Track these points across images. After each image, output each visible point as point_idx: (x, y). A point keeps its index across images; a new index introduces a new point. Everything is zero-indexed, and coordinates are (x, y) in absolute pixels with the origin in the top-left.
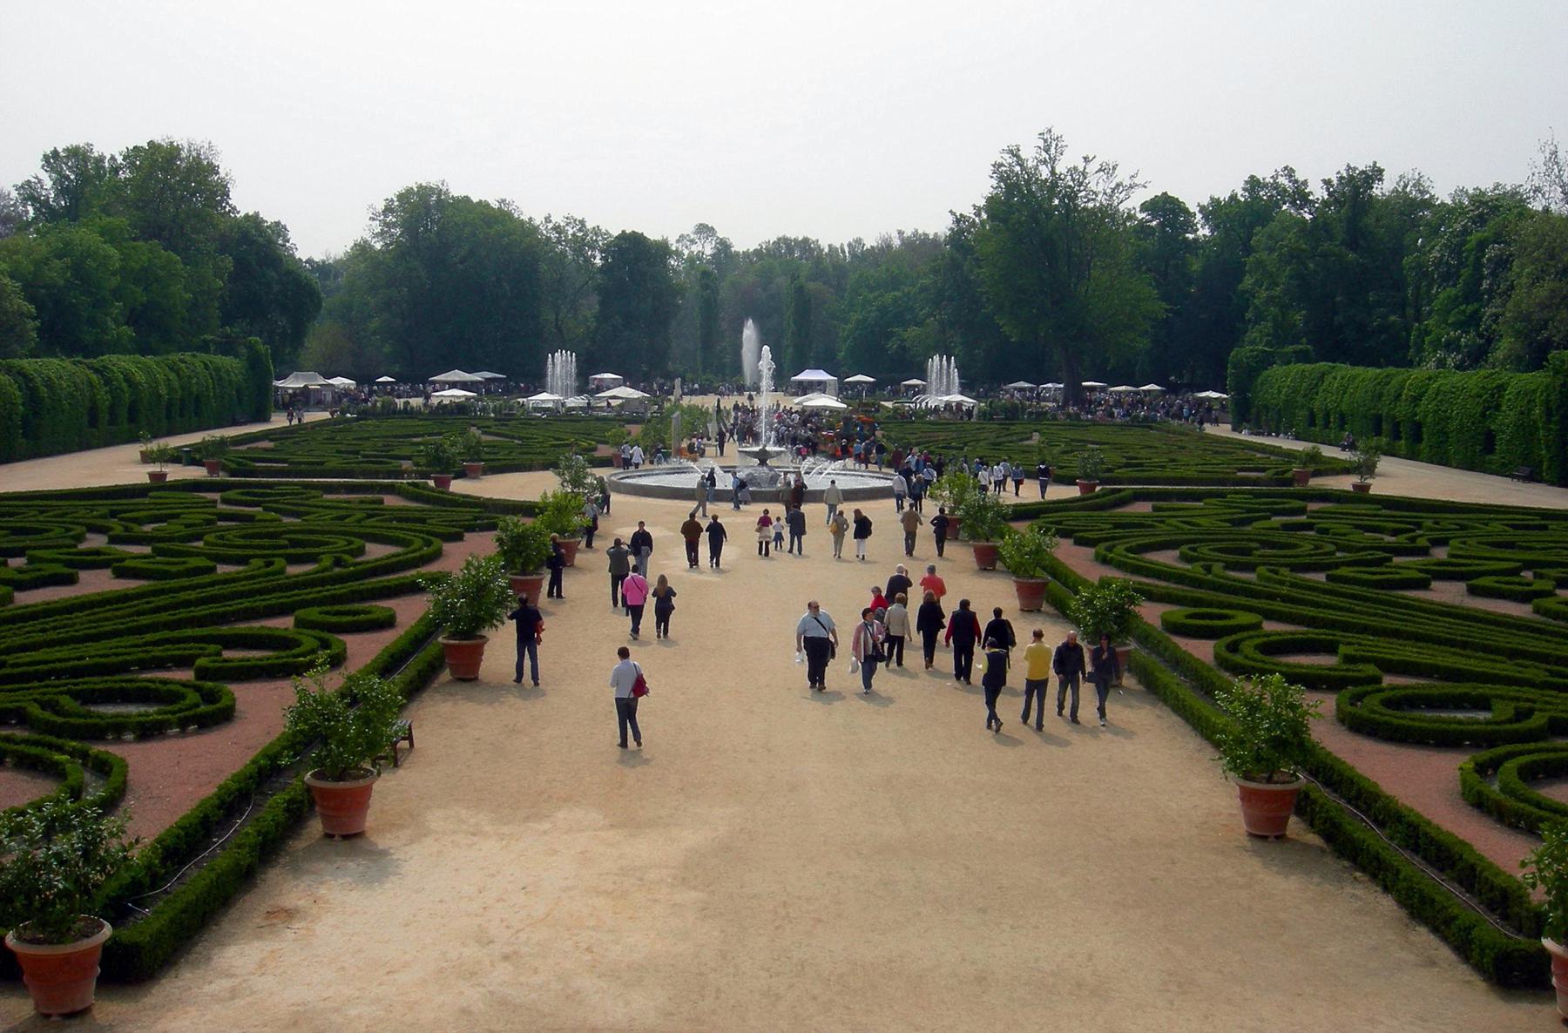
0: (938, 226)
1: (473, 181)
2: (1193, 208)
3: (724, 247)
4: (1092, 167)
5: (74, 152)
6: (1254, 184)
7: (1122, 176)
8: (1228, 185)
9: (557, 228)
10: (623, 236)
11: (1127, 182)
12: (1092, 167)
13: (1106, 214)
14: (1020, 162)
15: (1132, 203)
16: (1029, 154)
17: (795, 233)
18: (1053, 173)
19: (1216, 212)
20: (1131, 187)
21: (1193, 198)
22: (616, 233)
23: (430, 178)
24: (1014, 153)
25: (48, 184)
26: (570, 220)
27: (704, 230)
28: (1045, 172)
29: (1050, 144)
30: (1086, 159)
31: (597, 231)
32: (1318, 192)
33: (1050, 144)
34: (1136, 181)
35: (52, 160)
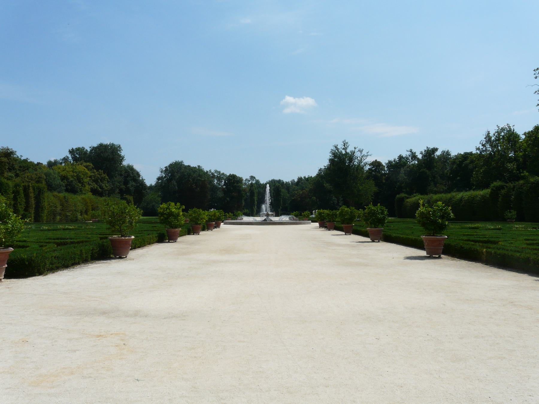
0: (314, 173)
1: (191, 161)
2: (384, 165)
3: (258, 182)
4: (357, 150)
5: (78, 149)
6: (401, 157)
7: (364, 153)
8: (393, 157)
9: (213, 174)
10: (230, 175)
11: (366, 154)
12: (357, 150)
13: (359, 168)
14: (338, 149)
16: (340, 146)
17: (277, 178)
18: (346, 152)
20: (367, 156)
21: (384, 161)
22: (228, 174)
23: (179, 159)
24: (336, 147)
25: (70, 158)
26: (216, 171)
27: (252, 178)
28: (344, 152)
29: (345, 144)
30: (355, 148)
31: (223, 174)
32: (420, 156)
33: (345, 144)
35: (72, 152)
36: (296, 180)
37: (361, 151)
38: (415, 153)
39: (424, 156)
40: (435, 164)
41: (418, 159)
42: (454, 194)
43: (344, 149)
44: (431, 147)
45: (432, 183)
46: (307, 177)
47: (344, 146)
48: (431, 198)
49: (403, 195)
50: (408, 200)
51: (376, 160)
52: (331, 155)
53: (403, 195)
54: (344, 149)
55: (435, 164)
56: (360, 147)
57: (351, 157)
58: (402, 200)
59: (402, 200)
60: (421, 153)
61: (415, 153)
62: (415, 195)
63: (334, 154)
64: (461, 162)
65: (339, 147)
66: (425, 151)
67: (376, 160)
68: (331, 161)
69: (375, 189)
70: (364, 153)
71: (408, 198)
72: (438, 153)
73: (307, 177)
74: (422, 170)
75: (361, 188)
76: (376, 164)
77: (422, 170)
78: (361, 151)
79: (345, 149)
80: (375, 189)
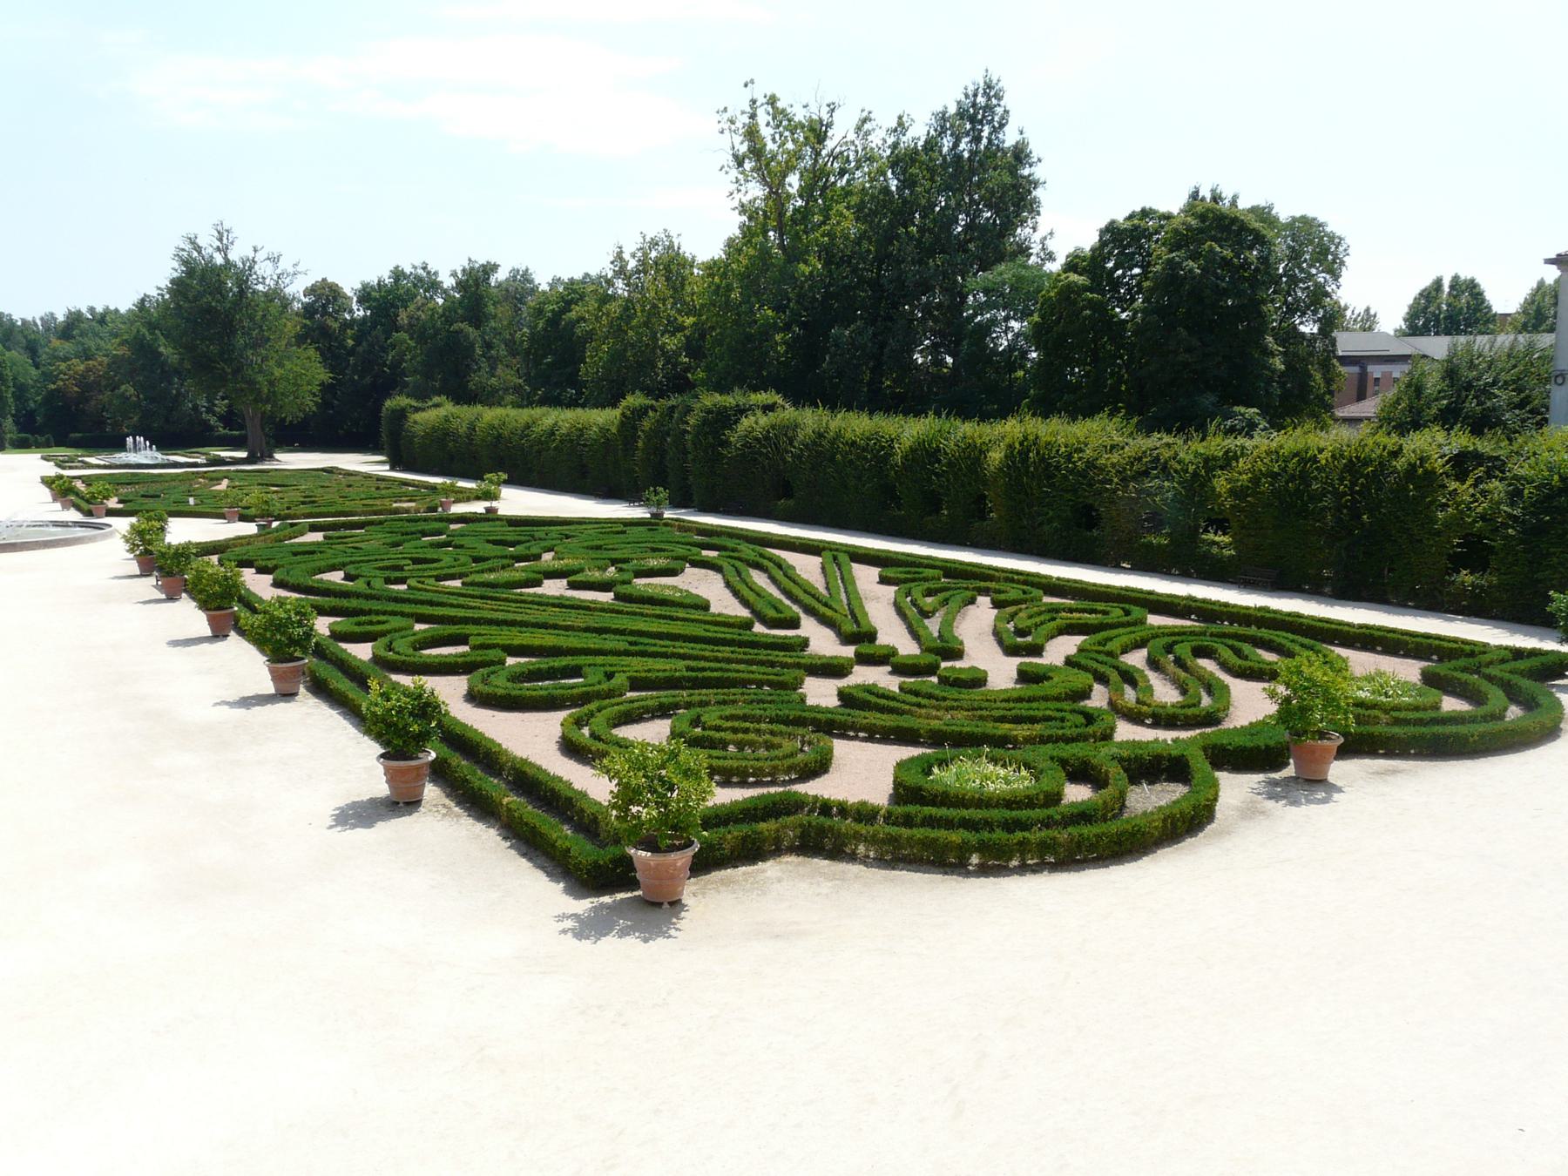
0: (125, 303)
2: (350, 294)
7: (284, 265)
8: (376, 271)
11: (291, 270)
13: (276, 296)
14: (198, 249)
15: (296, 289)
16: (207, 241)
19: (365, 295)
28: (219, 260)
29: (223, 237)
34: (299, 268)
36: (61, 318)
37: (275, 260)
38: (436, 273)
39: (461, 286)
40: (491, 309)
41: (445, 291)
42: (537, 412)
43: (218, 249)
44: (481, 260)
45: (485, 365)
46: (99, 309)
47: (221, 240)
48: (479, 417)
49: (401, 401)
50: (418, 417)
51: (324, 280)
52: (176, 264)
53: (401, 401)
54: (218, 249)
55: (491, 309)
56: (270, 248)
57: (243, 277)
58: (401, 414)
59: (401, 414)
60: (454, 274)
61: (436, 273)
62: (436, 399)
63: (185, 262)
64: (558, 315)
65: (200, 242)
66: (464, 270)
67: (324, 280)
68: (178, 287)
69: (323, 375)
70: (284, 265)
71: (417, 410)
72: (501, 275)
73: (99, 309)
74: (455, 327)
75: (278, 372)
76: (326, 296)
77: (455, 327)
78: (275, 260)
79: (223, 250)
80: (323, 375)
